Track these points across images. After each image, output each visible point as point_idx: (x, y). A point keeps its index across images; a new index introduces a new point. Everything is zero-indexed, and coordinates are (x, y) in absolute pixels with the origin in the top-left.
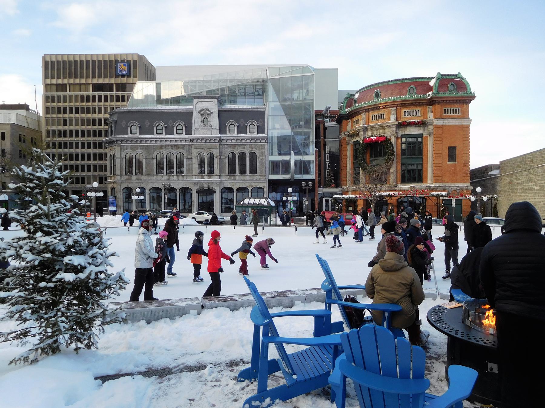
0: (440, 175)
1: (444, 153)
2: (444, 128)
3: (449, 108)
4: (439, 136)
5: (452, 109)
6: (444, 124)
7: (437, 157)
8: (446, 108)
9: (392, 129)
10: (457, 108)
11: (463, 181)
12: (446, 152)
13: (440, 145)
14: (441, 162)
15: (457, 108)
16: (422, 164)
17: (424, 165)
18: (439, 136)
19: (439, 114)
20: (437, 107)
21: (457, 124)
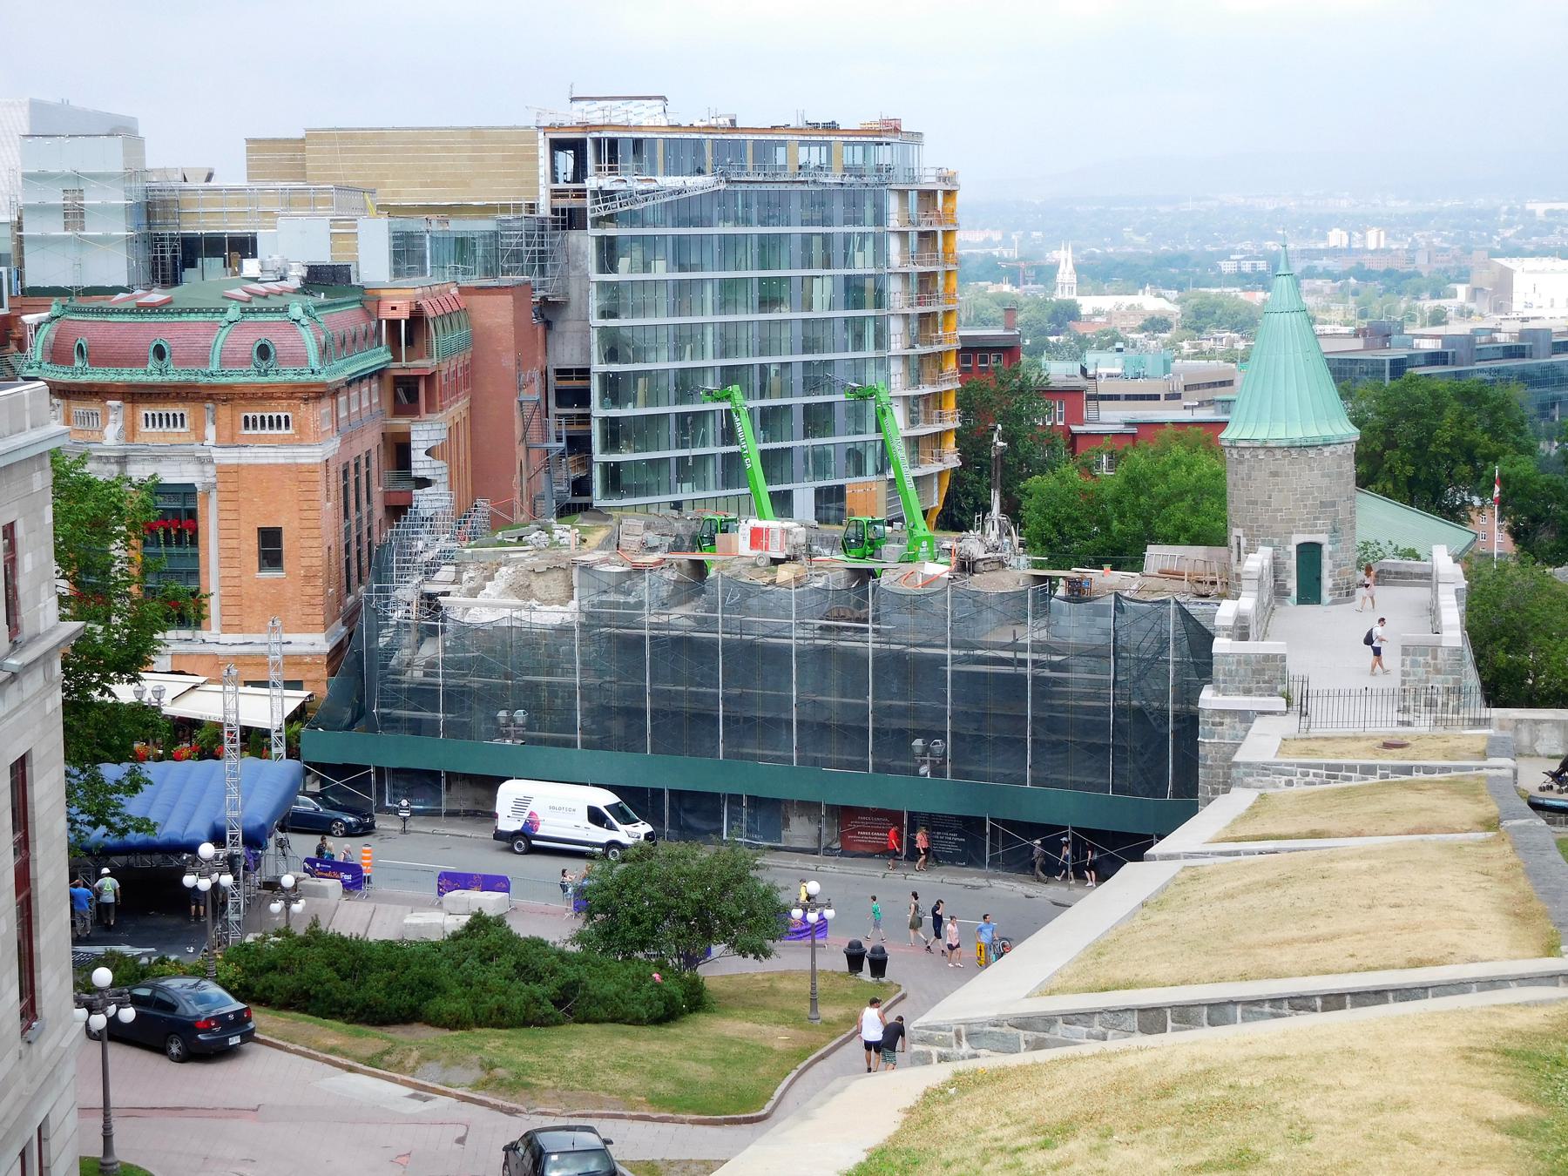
0: (235, 610)
1: (244, 547)
2: (244, 473)
3: (258, 415)
4: (230, 496)
5: (267, 416)
6: (242, 461)
7: (228, 557)
8: (250, 415)
9: (109, 467)
10: (282, 415)
11: (305, 627)
12: (252, 544)
13: (234, 525)
14: (236, 573)
15: (282, 415)
16: (194, 574)
17: (202, 577)
18: (230, 496)
19: (227, 433)
20: (224, 412)
21: (281, 461)
